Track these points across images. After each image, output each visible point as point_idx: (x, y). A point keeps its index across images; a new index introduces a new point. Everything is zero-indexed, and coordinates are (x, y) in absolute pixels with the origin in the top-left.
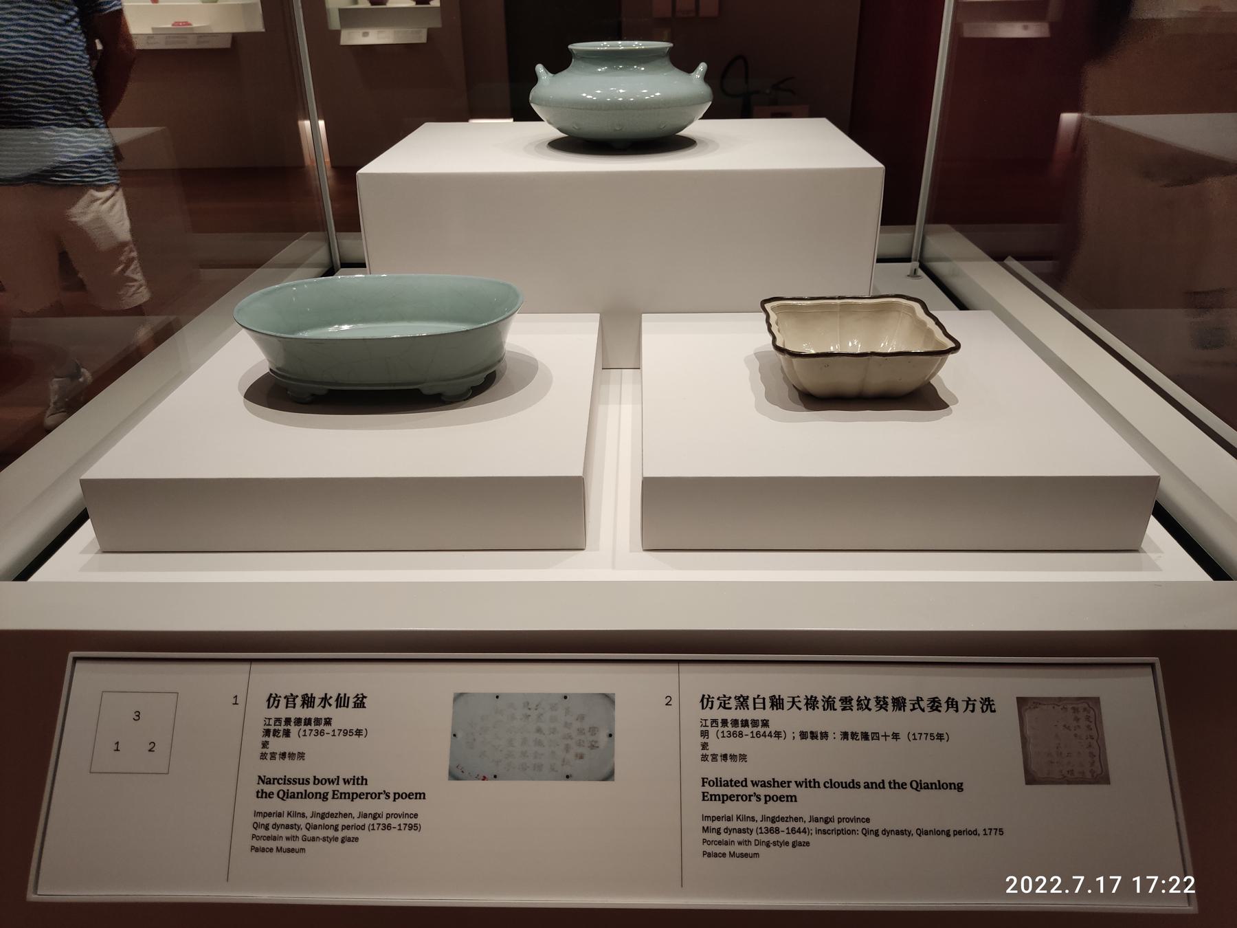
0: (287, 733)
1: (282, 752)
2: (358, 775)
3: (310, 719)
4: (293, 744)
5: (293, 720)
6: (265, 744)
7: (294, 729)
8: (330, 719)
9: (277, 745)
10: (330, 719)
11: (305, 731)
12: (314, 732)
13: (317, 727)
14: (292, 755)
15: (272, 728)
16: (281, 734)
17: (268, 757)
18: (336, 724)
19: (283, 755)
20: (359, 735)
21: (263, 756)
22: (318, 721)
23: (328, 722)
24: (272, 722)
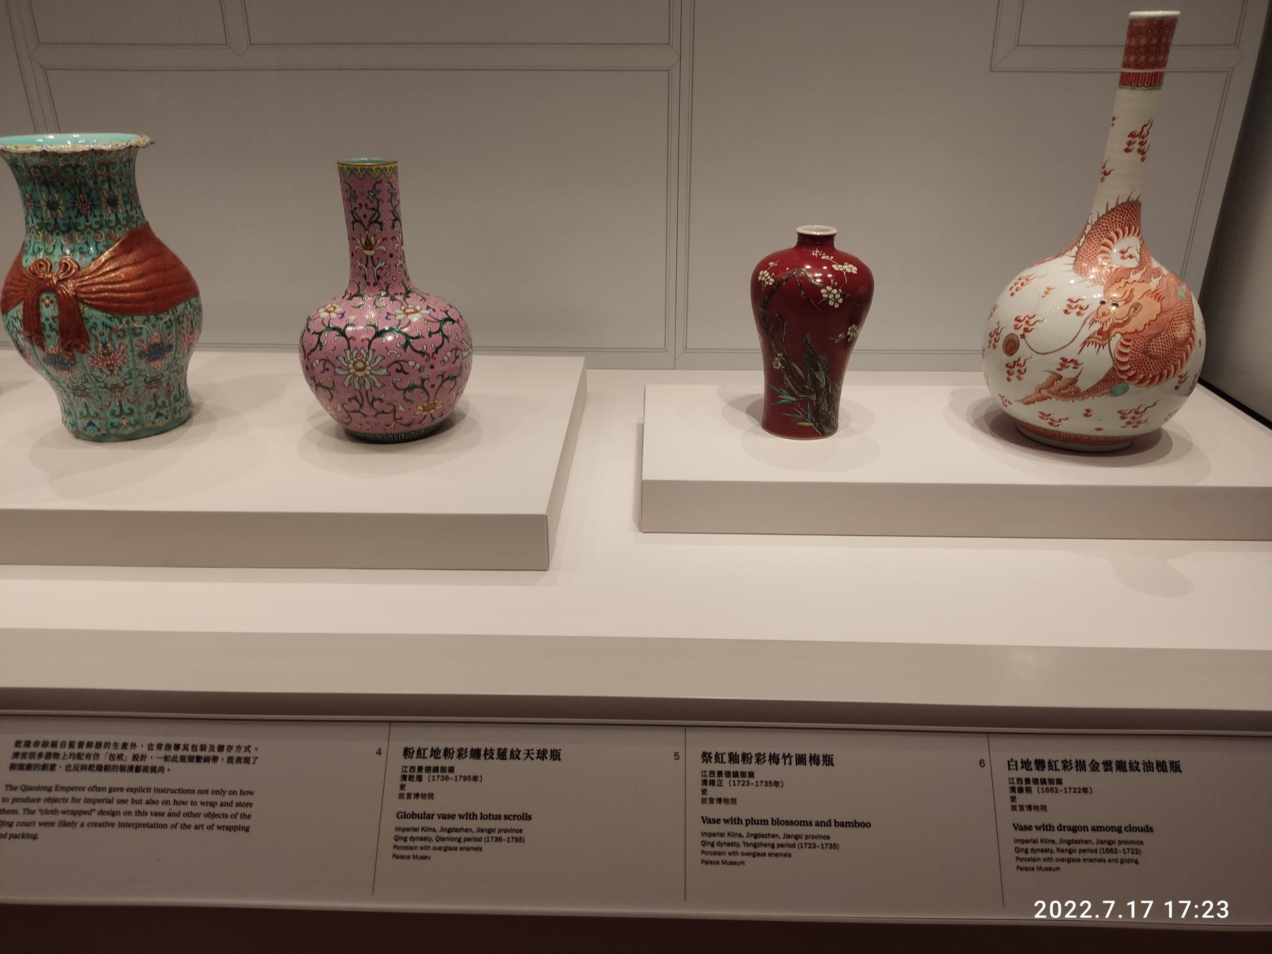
0: (420, 779)
1: (416, 792)
2: (470, 811)
3: (437, 768)
4: (423, 787)
5: (424, 768)
6: (402, 787)
7: (425, 775)
8: (453, 768)
9: (412, 787)
10: (453, 768)
11: (433, 777)
12: (440, 778)
13: (443, 774)
14: (424, 796)
15: (408, 774)
16: (415, 779)
17: (405, 796)
18: (457, 772)
19: (417, 795)
20: (476, 781)
21: (401, 796)
22: (443, 769)
23: (452, 770)
24: (408, 769)
